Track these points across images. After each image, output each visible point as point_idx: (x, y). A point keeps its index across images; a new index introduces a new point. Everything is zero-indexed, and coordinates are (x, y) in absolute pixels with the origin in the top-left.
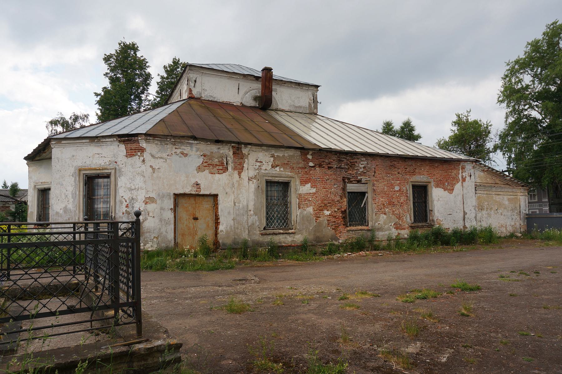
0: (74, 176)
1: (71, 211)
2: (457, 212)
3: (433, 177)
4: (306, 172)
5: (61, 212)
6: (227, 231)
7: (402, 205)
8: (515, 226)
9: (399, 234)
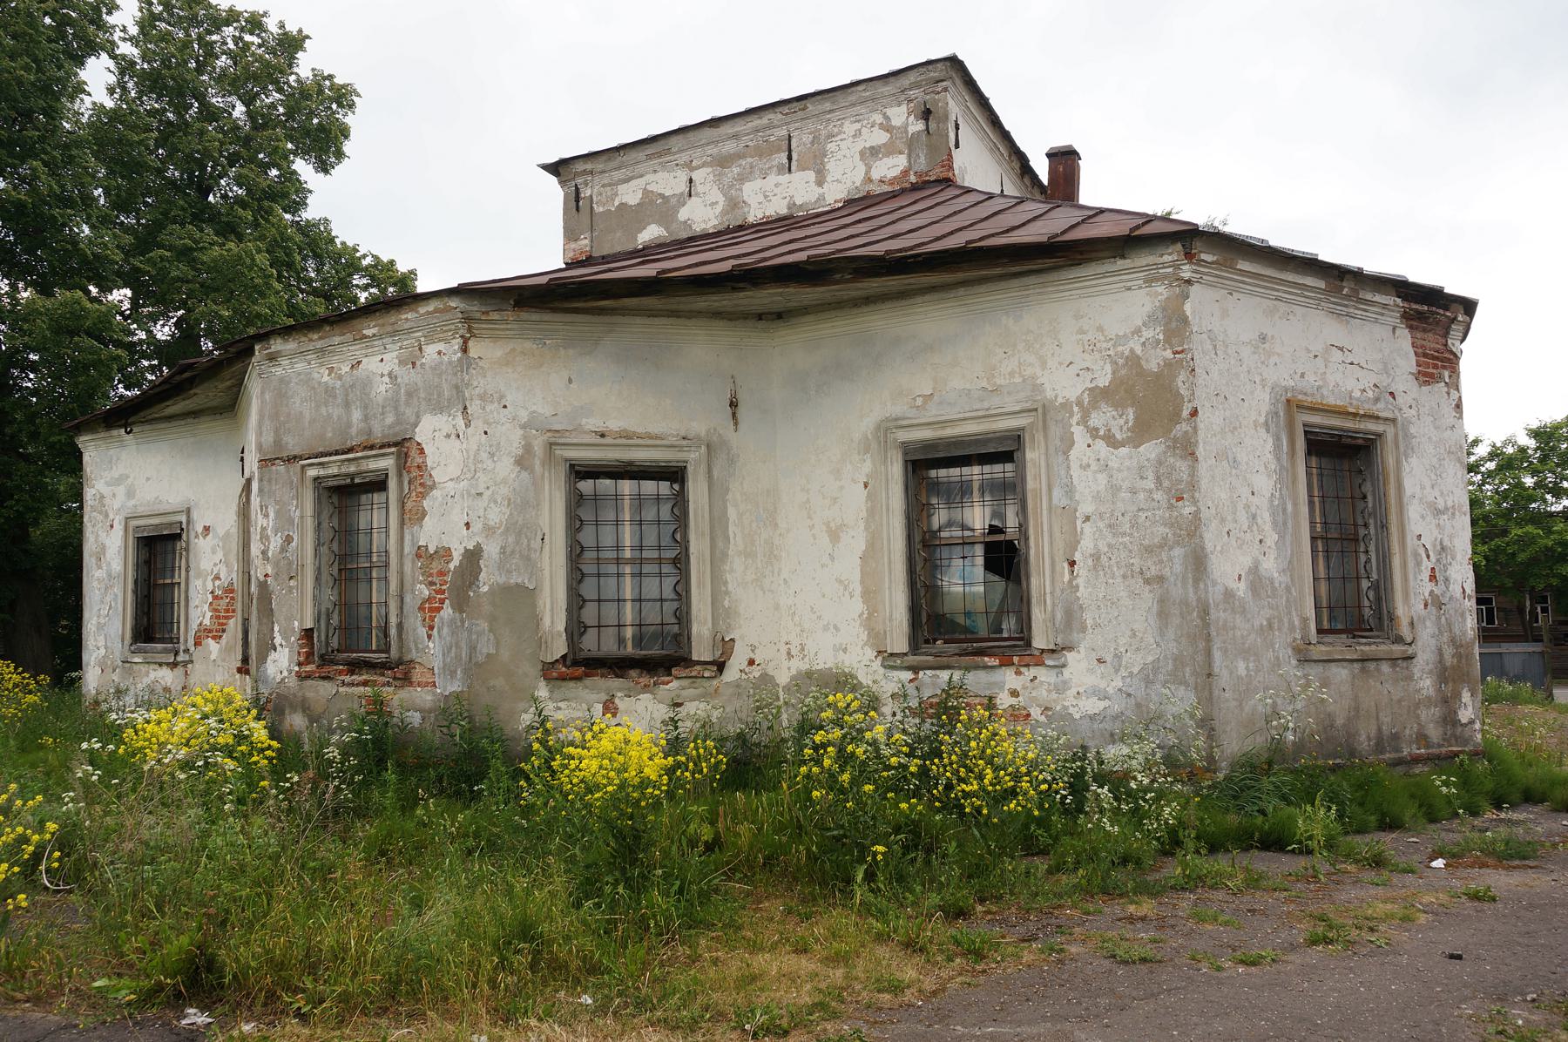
0: (1273, 427)
1: (1274, 589)
5: (1241, 589)
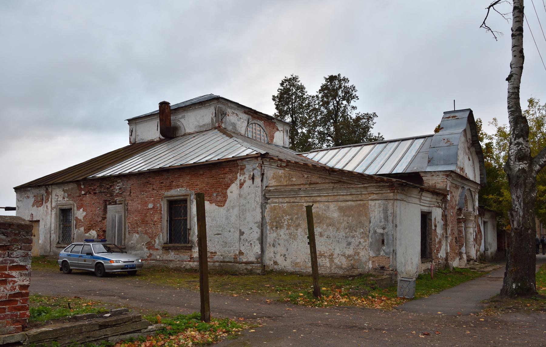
2: (230, 231)
3: (195, 187)
4: (81, 199)
6: (42, 244)
7: (156, 223)
8: (356, 257)
9: (151, 255)
